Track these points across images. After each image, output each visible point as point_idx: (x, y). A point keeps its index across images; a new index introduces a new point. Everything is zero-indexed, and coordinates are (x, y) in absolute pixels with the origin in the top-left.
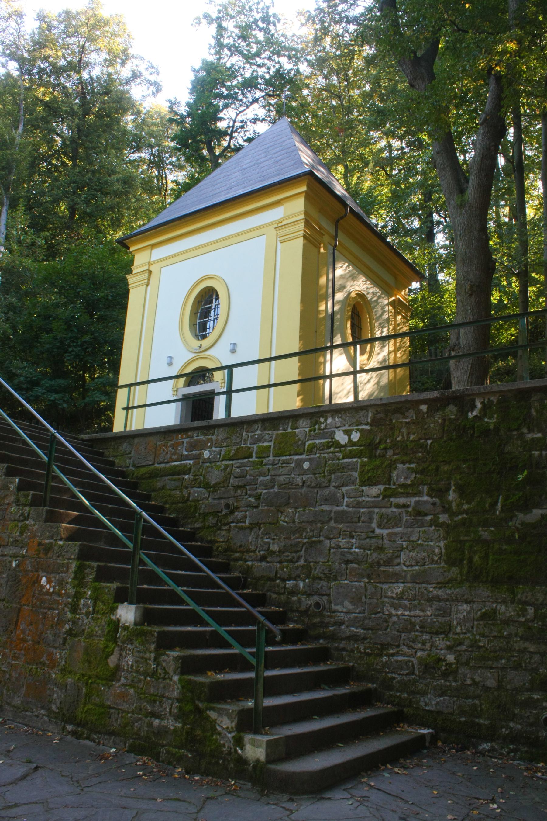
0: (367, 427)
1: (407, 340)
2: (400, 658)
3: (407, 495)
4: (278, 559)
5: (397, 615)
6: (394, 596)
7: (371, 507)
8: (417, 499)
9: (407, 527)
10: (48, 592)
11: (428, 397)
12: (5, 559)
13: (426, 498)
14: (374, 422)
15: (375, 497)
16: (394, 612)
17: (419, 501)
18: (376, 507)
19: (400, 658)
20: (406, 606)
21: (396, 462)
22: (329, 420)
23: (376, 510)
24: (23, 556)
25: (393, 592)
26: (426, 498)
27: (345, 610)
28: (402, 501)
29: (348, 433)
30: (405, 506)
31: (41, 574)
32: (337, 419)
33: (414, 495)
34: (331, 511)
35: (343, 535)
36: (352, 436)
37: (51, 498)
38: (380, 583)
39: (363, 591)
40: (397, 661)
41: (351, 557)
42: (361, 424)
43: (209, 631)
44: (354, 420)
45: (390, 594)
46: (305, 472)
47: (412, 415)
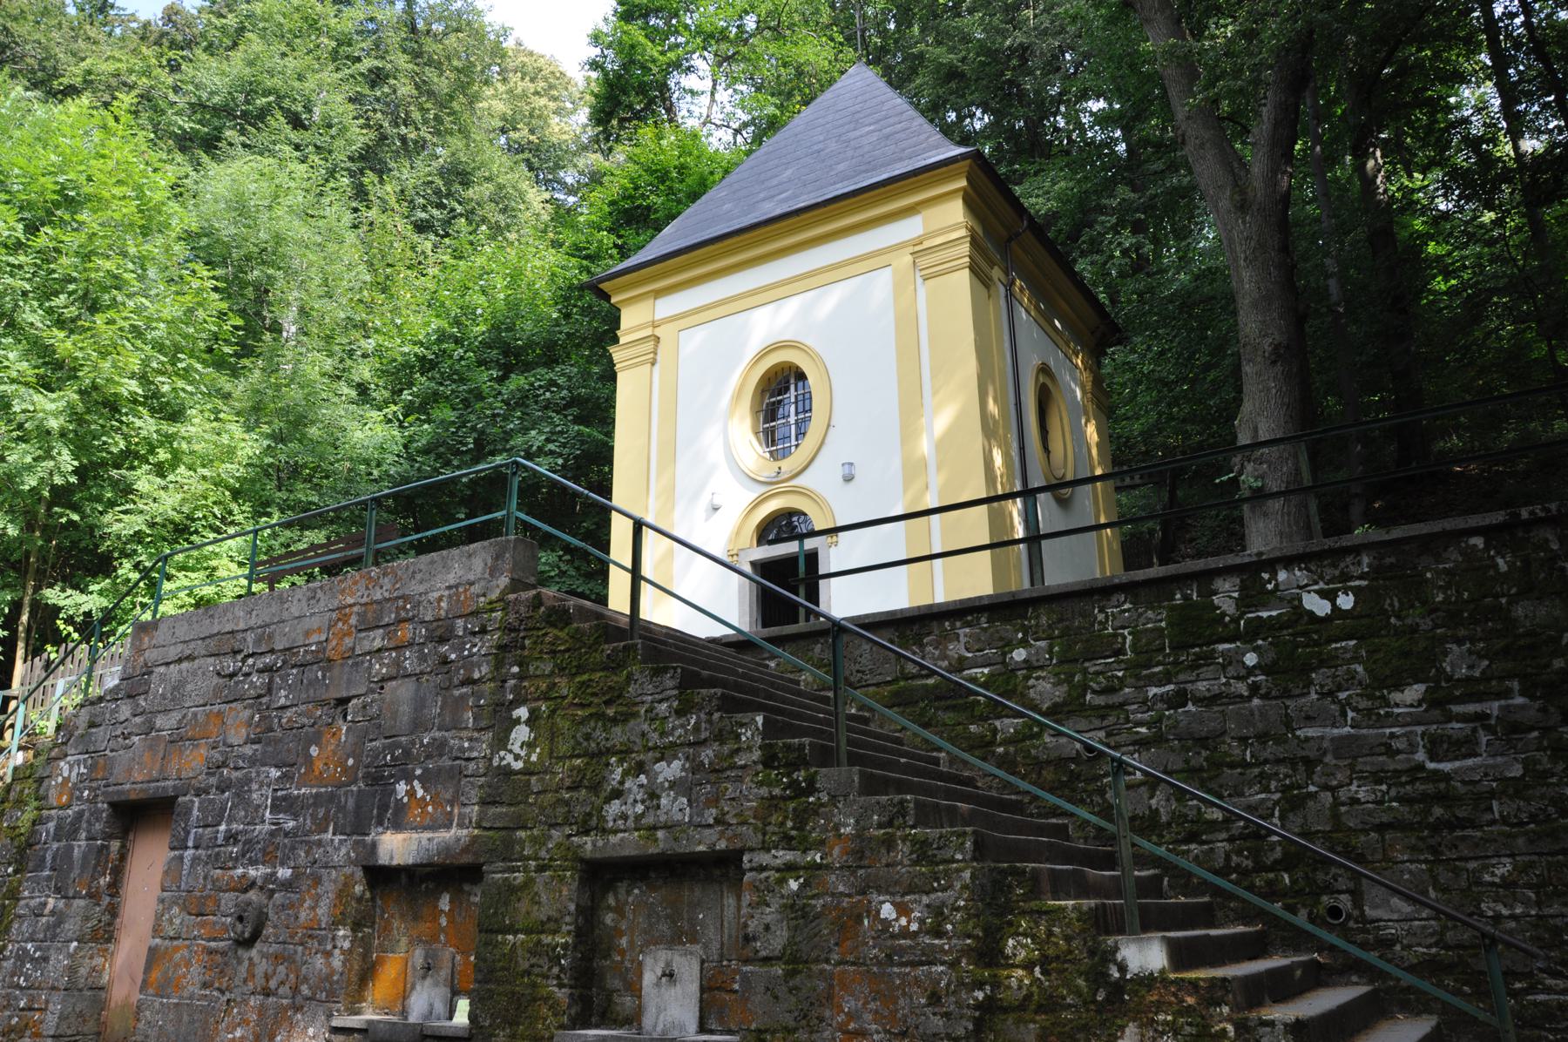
0: (1364, 583)
1: (1244, 439)
2: (1541, 997)
3: (1479, 697)
4: (1224, 835)
5: (1513, 917)
6: (1497, 880)
7: (1408, 725)
8: (1503, 702)
9: (1494, 756)
10: (905, 933)
11: (1487, 522)
12: (765, 874)
13: (1519, 700)
14: (1376, 573)
15: (1412, 706)
16: (1505, 912)
17: (1508, 706)
18: (1419, 724)
19: (1541, 997)
20: (1529, 898)
21: (1443, 640)
22: (1282, 576)
23: (1420, 729)
24: (814, 866)
25: (1493, 874)
26: (1519, 700)
27: (1395, 917)
28: (1471, 708)
29: (1329, 595)
30: (1481, 717)
31: (876, 897)
32: (1298, 573)
33: (1499, 696)
34: (1322, 738)
35: (1359, 779)
36: (1339, 601)
37: (849, 753)
38: (1460, 859)
39: (1426, 877)
40: (1536, 1004)
41: (1385, 819)
42: (1352, 578)
43: (1235, 978)
44: (1337, 573)
45: (1487, 878)
46: (1251, 671)
47: (1453, 557)
